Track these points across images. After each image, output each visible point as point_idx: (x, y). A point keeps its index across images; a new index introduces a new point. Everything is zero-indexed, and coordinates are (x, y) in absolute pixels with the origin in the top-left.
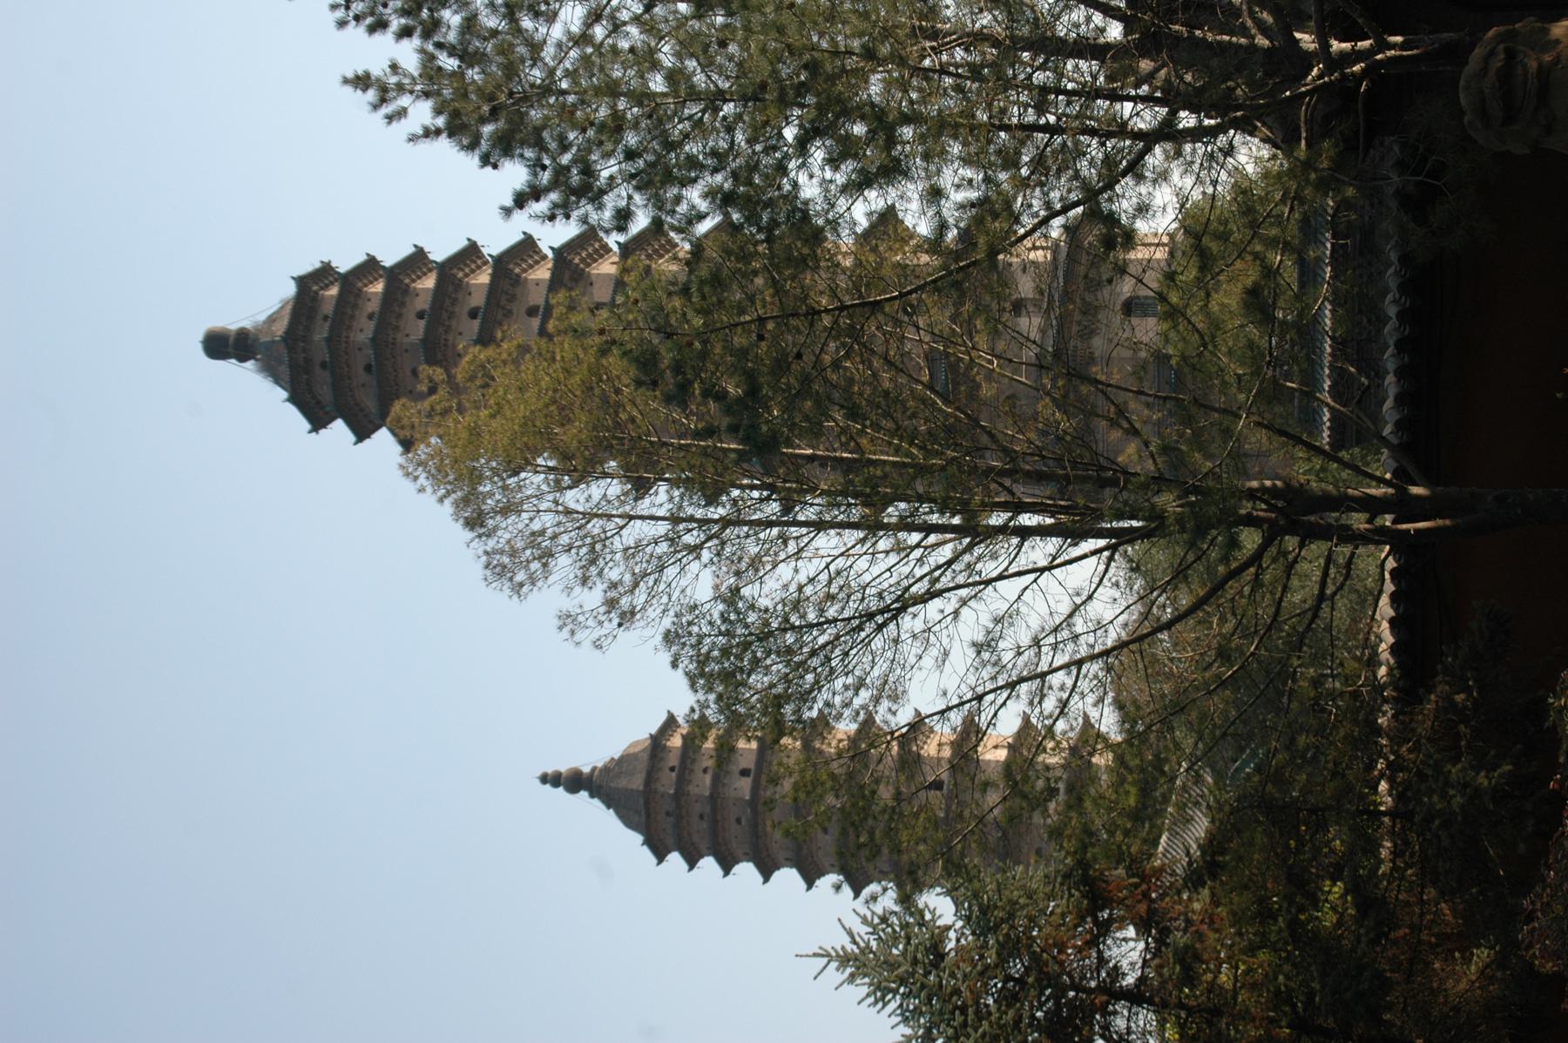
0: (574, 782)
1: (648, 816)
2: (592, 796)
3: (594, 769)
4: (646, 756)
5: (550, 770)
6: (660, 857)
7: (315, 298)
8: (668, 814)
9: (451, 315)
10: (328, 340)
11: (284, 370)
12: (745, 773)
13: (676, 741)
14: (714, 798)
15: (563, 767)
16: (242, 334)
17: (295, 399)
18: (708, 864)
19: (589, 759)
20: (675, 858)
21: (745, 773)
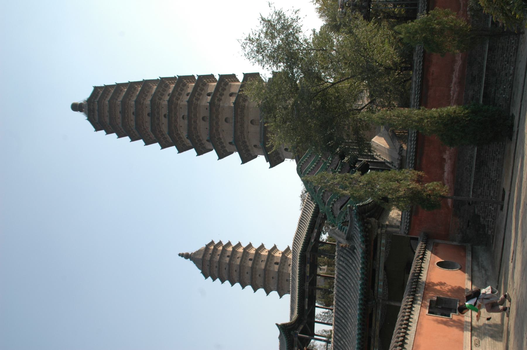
1: (203, 265)
2: (191, 260)
5: (181, 253)
6: (206, 277)
7: (98, 93)
9: (131, 96)
10: (98, 102)
11: (87, 112)
12: (228, 256)
13: (212, 247)
14: (219, 262)
15: (184, 252)
16: (81, 104)
17: (89, 119)
19: (191, 250)
20: (210, 278)
21: (228, 256)
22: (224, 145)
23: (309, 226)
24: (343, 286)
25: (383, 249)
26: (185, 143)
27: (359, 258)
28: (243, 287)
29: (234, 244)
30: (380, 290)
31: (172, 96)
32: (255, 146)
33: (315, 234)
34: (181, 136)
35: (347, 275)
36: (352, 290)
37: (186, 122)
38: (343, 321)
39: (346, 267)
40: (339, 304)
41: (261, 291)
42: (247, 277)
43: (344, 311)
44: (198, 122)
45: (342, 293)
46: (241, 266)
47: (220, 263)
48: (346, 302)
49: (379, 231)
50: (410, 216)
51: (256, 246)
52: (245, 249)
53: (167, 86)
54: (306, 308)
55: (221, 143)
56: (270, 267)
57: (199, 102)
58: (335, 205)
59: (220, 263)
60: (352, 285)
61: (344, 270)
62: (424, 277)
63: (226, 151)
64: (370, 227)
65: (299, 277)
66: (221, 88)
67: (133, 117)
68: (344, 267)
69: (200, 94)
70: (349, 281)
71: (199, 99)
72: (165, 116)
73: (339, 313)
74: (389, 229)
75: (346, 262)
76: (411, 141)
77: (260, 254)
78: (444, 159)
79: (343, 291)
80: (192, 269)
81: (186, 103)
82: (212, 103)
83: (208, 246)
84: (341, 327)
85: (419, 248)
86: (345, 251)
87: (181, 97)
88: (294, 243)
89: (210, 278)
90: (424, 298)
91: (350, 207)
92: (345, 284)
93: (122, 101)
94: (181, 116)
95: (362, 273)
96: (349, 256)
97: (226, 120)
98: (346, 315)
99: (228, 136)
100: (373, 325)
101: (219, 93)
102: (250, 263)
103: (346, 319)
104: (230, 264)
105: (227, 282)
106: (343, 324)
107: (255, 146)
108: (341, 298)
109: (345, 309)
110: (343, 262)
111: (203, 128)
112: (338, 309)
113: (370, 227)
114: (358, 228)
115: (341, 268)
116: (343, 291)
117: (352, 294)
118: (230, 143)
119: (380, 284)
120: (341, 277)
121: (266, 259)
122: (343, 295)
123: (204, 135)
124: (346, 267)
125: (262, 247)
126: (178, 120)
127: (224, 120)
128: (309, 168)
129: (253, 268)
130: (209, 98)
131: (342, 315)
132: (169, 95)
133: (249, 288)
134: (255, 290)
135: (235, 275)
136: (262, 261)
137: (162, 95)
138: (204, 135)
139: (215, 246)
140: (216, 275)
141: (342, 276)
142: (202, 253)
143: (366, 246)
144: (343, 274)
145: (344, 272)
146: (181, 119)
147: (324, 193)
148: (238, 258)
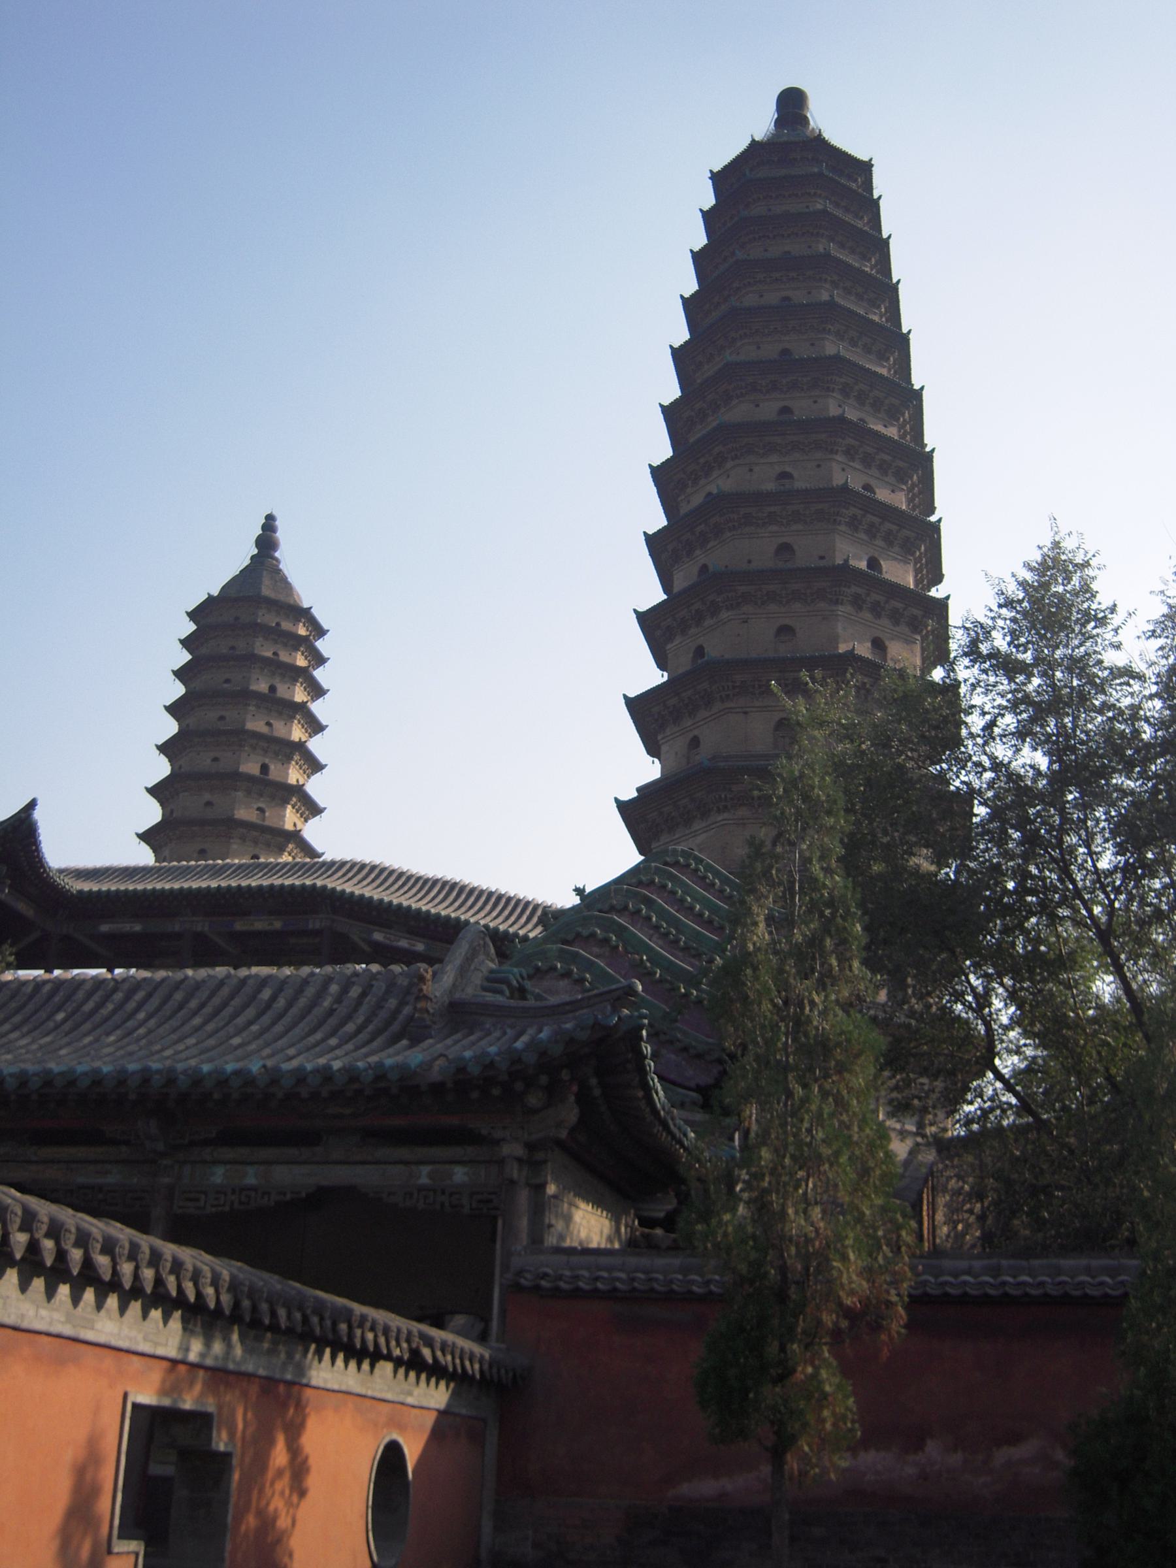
0: (267, 542)
2: (253, 558)
3: (277, 560)
4: (292, 602)
5: (278, 523)
8: (237, 618)
12: (273, 689)
13: (302, 631)
14: (252, 659)
15: (280, 535)
16: (805, 121)
17: (754, 147)
18: (185, 657)
20: (192, 627)
21: (273, 689)
22: (693, 631)
23: (438, 915)
24: (225, 1004)
25: (424, 1174)
26: (689, 490)
27: (373, 1059)
28: (164, 748)
29: (318, 708)
30: (218, 1175)
31: (861, 431)
32: (695, 742)
33: (403, 943)
34: (715, 474)
35: (281, 1016)
36: (211, 1042)
37: (770, 486)
38: (60, 1016)
39: (318, 1012)
40: (140, 995)
41: (152, 813)
42: (203, 761)
43: (106, 1019)
44: (774, 528)
45: (193, 1004)
46: (240, 738)
47: (248, 661)
48: (152, 1023)
49: (513, 1149)
50: (612, 1295)
51: (315, 787)
52: (301, 747)
53: (892, 416)
54: (105, 928)
55: (699, 618)
56: (243, 839)
57: (843, 528)
58: (563, 984)
59: (248, 661)
60: (236, 1041)
61: (302, 1002)
62: (329, 1374)
63: (670, 639)
64: (533, 1100)
65: (229, 888)
66: (899, 605)
67: (772, 298)
68: (314, 1003)
69: (872, 531)
70: (255, 1028)
71: (856, 529)
72: (786, 410)
73: (96, 998)
74: (523, 1197)
75: (342, 1010)
76: (996, 1271)
77: (285, 802)
78: (919, 1446)
79: (203, 1005)
80: (220, 564)
81: (838, 480)
82: (845, 573)
83: (305, 615)
84: (30, 1007)
85: (454, 1342)
86: (392, 1003)
87: (857, 465)
88: (363, 866)
89: (192, 627)
90: (219, 1376)
91: (631, 990)
92: (236, 1014)
93: (827, 255)
94: (788, 469)
95: (300, 1076)
96: (368, 1021)
97: (785, 631)
98: (88, 1026)
99: (721, 639)
100: (48, 1152)
101: (881, 599)
102: (251, 767)
103: (67, 1026)
104: (245, 696)
105: (178, 690)
106: (43, 1014)
107: (695, 742)
108: (164, 1002)
109: (117, 1018)
110: (339, 1000)
111: (752, 549)
112: (115, 990)
113: (533, 1100)
114: (525, 1038)
115: (310, 991)
116: (203, 1005)
117: (191, 1041)
118: (700, 651)
119: (251, 1170)
120: (266, 994)
121: (267, 823)
122: (181, 1007)
123: (721, 555)
124: (318, 1012)
125: (312, 809)
126: (774, 458)
127: (787, 622)
128: (687, 890)
129: (235, 777)
130: (863, 565)
131: (87, 1007)
132: (861, 420)
133: (162, 768)
134: (154, 791)
135: (208, 716)
136: (261, 810)
137: (861, 399)
138: (721, 555)
139: (305, 640)
140: (204, 651)
141: (274, 998)
142: (282, 597)
143: (438, 1088)
144: (281, 1002)
145: (290, 1005)
146: (778, 469)
147: (606, 941)
148: (269, 724)
